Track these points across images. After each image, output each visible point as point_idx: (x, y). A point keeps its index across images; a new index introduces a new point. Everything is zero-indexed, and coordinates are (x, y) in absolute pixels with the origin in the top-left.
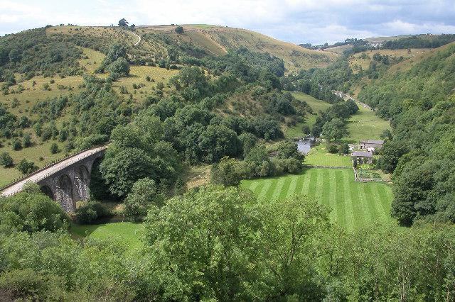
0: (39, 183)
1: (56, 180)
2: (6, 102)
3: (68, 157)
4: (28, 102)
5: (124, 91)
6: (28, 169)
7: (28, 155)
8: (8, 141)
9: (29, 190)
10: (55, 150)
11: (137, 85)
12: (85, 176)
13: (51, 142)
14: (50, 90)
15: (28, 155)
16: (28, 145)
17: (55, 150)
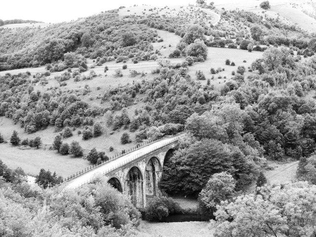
1: (126, 171)
2: (77, 89)
4: (99, 89)
5: (201, 77)
6: (96, 159)
7: (98, 145)
8: (78, 130)
10: (125, 141)
11: (215, 69)
12: (157, 169)
14: (122, 76)
15: (98, 145)
16: (98, 133)
17: (125, 141)
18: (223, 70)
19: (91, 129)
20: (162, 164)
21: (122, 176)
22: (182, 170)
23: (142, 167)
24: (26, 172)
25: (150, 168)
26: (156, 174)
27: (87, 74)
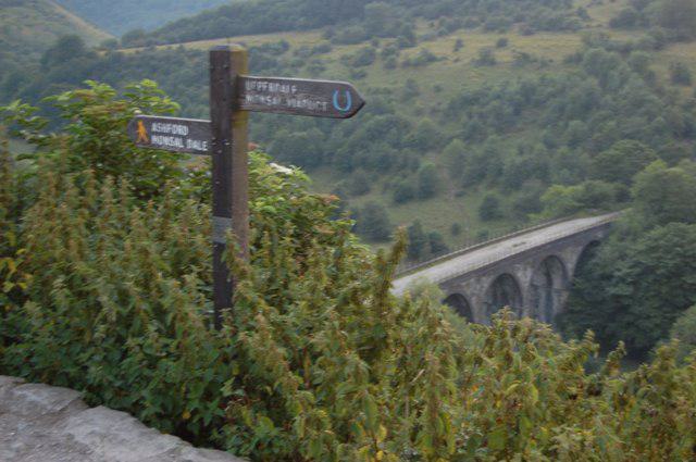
0: (444, 284)
1: (487, 282)
2: (390, 87)
4: (438, 89)
7: (431, 217)
8: (384, 179)
10: (489, 213)
12: (557, 283)
13: (485, 192)
15: (431, 217)
16: (427, 192)
17: (489, 213)
19: (412, 181)
20: (570, 273)
21: (476, 292)
22: (617, 297)
23: (524, 276)
25: (541, 281)
26: (555, 296)
27: (413, 53)
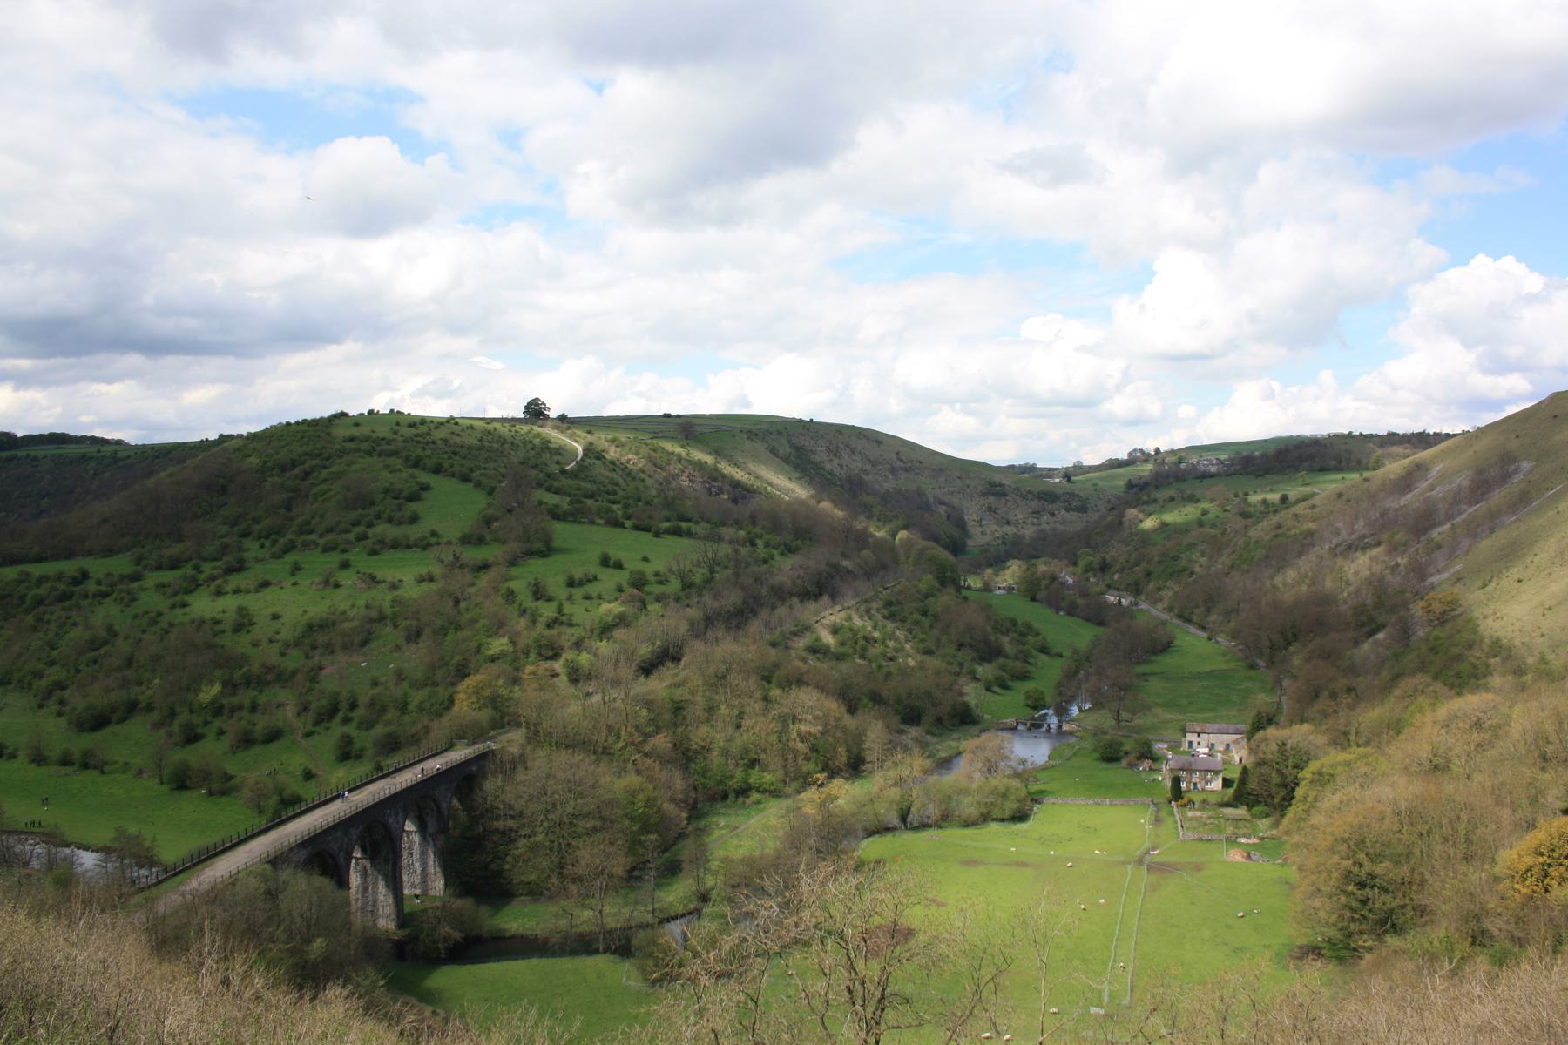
1: (355, 833)
3: (381, 773)
4: (276, 617)
5: (539, 593)
9: (276, 861)
13: (337, 730)
14: (337, 586)
17: (346, 753)
18: (595, 578)
24: (71, 836)
